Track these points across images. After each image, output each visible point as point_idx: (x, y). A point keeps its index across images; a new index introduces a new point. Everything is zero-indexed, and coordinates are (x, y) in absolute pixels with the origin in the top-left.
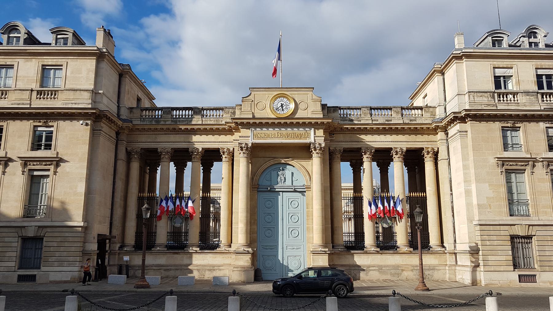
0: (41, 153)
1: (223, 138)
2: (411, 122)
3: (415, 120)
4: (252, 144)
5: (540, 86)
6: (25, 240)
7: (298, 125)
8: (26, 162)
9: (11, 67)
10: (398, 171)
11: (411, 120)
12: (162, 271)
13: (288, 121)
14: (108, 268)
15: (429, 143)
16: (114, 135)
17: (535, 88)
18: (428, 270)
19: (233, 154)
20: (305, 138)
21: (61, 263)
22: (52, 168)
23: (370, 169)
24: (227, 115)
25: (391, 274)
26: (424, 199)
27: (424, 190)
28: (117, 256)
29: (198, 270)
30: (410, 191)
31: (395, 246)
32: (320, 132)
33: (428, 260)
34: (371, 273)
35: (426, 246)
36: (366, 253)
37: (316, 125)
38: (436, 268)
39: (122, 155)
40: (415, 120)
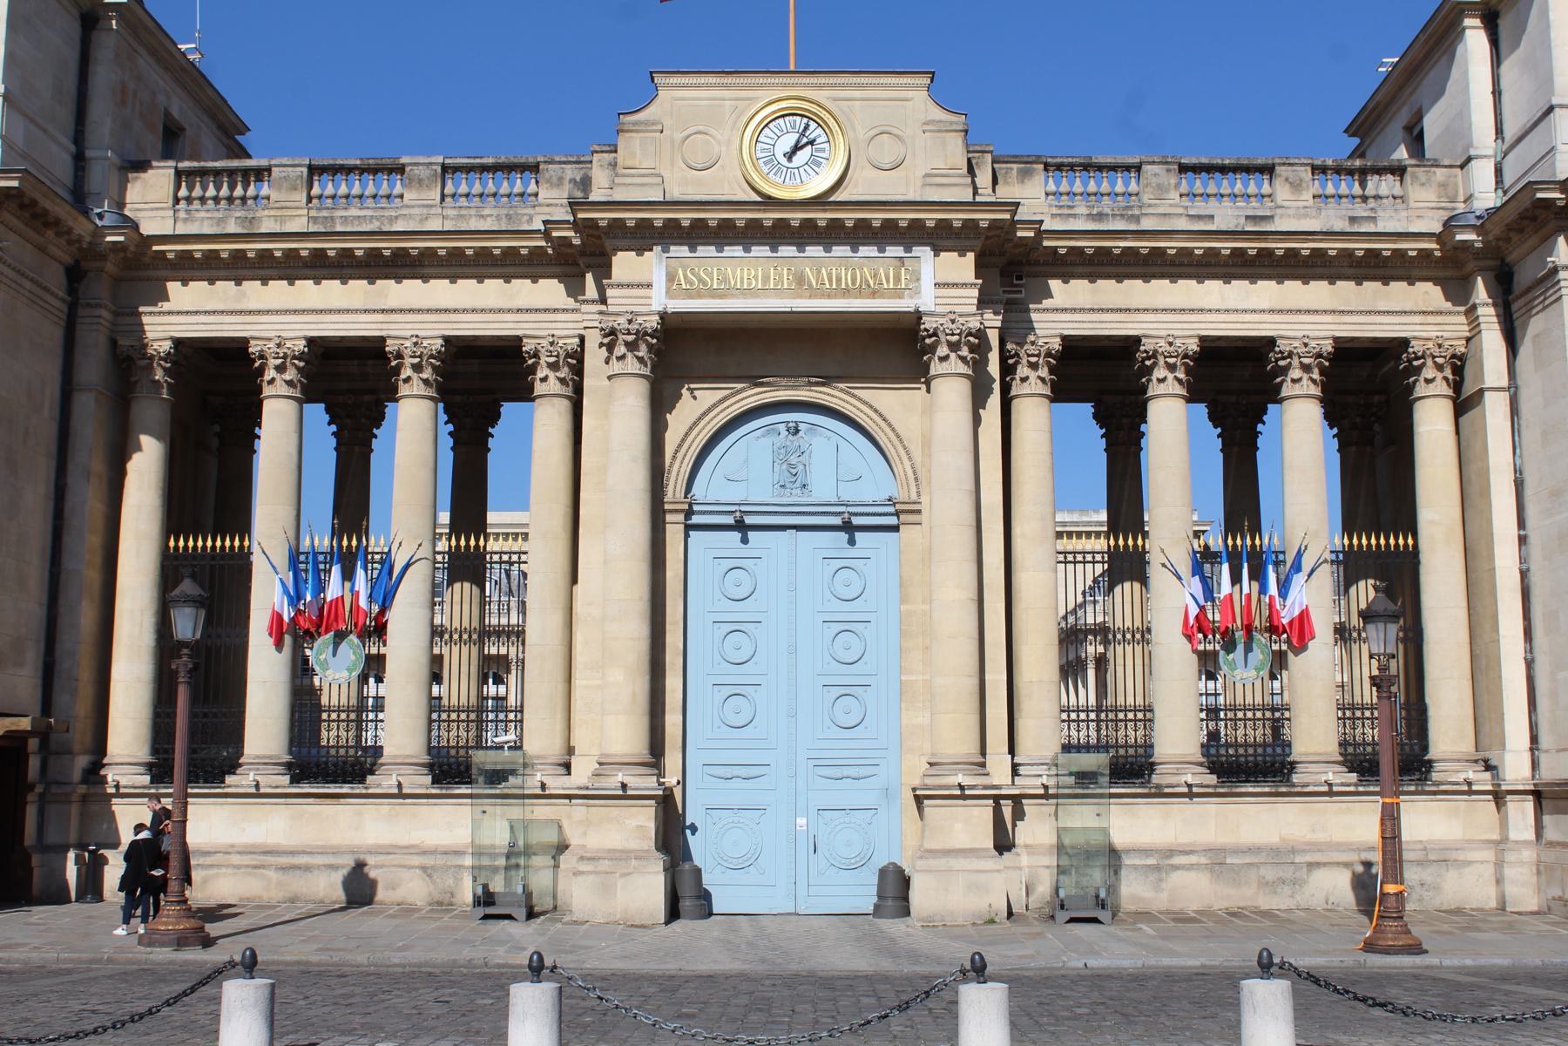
2: (1356, 229)
3: (1373, 219)
4: (663, 316)
7: (860, 234)
10: (1300, 438)
11: (1353, 220)
12: (272, 874)
13: (822, 217)
14: (36, 860)
15: (1430, 319)
16: (55, 279)
18: (1420, 863)
19: (581, 361)
20: (897, 293)
23: (1173, 427)
24: (554, 193)
25: (1264, 884)
26: (1411, 560)
27: (1407, 521)
28: (75, 809)
29: (424, 868)
30: (1349, 526)
31: (1283, 765)
32: (962, 266)
33: (1424, 821)
34: (1177, 878)
35: (1414, 765)
36: (1159, 793)
37: (941, 237)
38: (1453, 855)
39: (93, 368)
40: (1373, 219)
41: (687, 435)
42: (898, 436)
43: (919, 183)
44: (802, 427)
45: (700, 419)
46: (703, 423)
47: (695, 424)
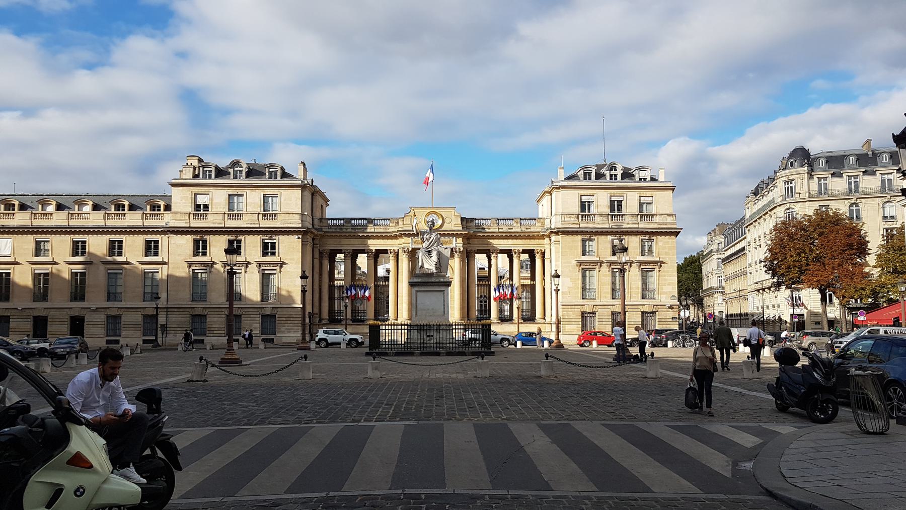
0: (269, 258)
1: (390, 242)
5: (612, 210)
6: (264, 316)
8: (260, 264)
9: (242, 195)
17: (608, 211)
21: (289, 331)
22: (278, 268)
32: (460, 240)
37: (457, 236)
39: (317, 255)
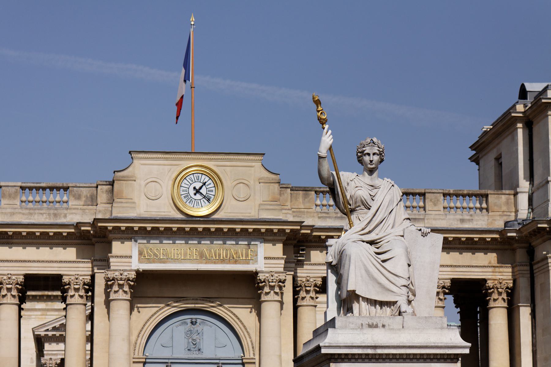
41: (144, 325)
42: (244, 327)
43: (257, 208)
44: (198, 321)
45: (150, 318)
46: (152, 320)
47: (148, 320)
